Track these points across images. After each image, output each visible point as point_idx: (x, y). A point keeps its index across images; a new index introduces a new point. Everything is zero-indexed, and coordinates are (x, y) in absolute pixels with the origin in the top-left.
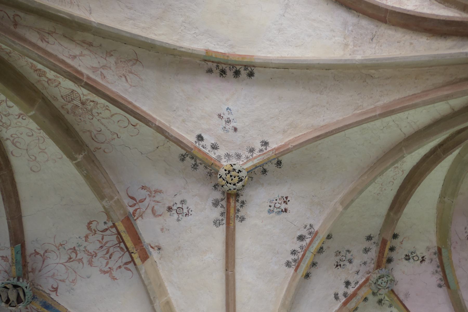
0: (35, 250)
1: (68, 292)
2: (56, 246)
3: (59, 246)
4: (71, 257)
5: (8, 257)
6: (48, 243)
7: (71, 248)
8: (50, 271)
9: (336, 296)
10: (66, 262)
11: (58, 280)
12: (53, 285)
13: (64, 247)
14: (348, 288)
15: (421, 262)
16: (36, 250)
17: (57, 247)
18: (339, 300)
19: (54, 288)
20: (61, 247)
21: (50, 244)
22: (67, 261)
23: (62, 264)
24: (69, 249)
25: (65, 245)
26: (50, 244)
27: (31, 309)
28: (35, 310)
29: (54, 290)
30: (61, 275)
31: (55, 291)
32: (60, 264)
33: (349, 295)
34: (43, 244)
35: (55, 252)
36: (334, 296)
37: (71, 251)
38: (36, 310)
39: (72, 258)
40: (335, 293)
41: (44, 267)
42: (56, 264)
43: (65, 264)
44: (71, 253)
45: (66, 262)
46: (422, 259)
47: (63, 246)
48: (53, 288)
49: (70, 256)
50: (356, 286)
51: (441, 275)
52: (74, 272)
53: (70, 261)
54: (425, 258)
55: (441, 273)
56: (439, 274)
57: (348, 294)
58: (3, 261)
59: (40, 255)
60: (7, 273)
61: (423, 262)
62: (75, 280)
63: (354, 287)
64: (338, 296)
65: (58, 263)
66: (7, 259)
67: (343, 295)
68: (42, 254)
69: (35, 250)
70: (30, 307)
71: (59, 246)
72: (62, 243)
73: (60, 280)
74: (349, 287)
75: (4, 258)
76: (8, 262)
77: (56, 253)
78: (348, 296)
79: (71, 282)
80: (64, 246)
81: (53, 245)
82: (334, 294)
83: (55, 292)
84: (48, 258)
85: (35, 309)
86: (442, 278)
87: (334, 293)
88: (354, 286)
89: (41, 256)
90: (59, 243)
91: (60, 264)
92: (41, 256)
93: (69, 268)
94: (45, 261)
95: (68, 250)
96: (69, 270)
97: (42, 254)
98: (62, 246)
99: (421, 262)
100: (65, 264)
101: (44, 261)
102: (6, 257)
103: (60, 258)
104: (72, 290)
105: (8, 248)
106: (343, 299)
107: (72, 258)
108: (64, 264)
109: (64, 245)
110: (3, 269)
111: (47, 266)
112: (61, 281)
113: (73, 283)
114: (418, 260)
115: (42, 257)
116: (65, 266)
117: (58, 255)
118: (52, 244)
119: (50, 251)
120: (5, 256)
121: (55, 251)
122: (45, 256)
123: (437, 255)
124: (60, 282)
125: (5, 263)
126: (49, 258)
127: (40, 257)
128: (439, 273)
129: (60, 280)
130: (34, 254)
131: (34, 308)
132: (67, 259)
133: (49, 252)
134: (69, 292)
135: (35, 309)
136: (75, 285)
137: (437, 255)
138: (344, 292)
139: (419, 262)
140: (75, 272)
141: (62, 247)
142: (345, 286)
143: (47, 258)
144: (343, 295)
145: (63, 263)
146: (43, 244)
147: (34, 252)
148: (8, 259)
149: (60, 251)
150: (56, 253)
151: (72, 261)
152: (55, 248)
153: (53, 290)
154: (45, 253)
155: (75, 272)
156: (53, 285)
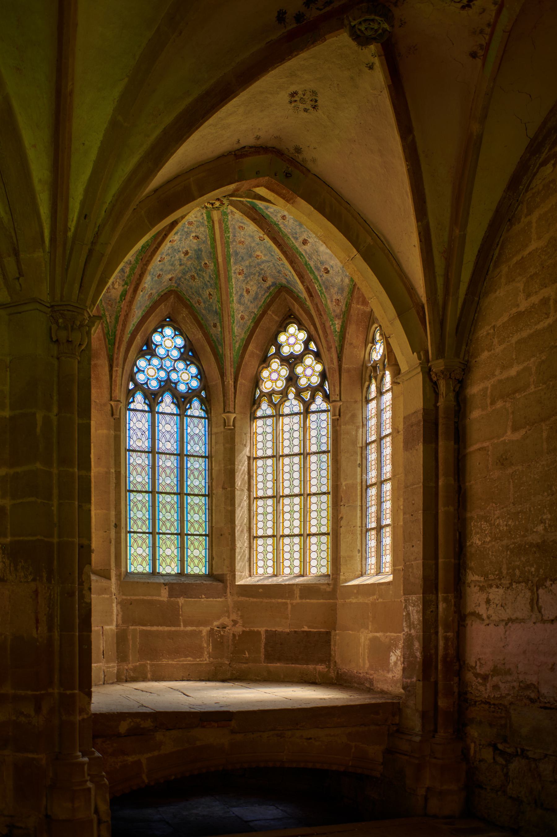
9: (281, 16)
14: (308, 8)
15: (463, 7)
18: (284, 24)
33: (305, 22)
36: (276, 14)
40: (280, 10)
46: (467, 3)
50: (324, 8)
51: (485, 39)
54: (474, 4)
55: (487, 37)
56: (484, 37)
57: (305, 17)
61: (467, 8)
63: (321, 10)
64: (284, 16)
67: (295, 17)
74: (311, 6)
78: (303, 23)
82: (278, 12)
86: (485, 45)
87: (279, 10)
88: (322, 7)
99: (463, 7)
106: (292, 25)
114: (459, 2)
123: (497, 6)
128: (485, 35)
137: (497, 6)
138: (298, 13)
139: (460, 5)
142: (304, 3)
144: (295, 17)
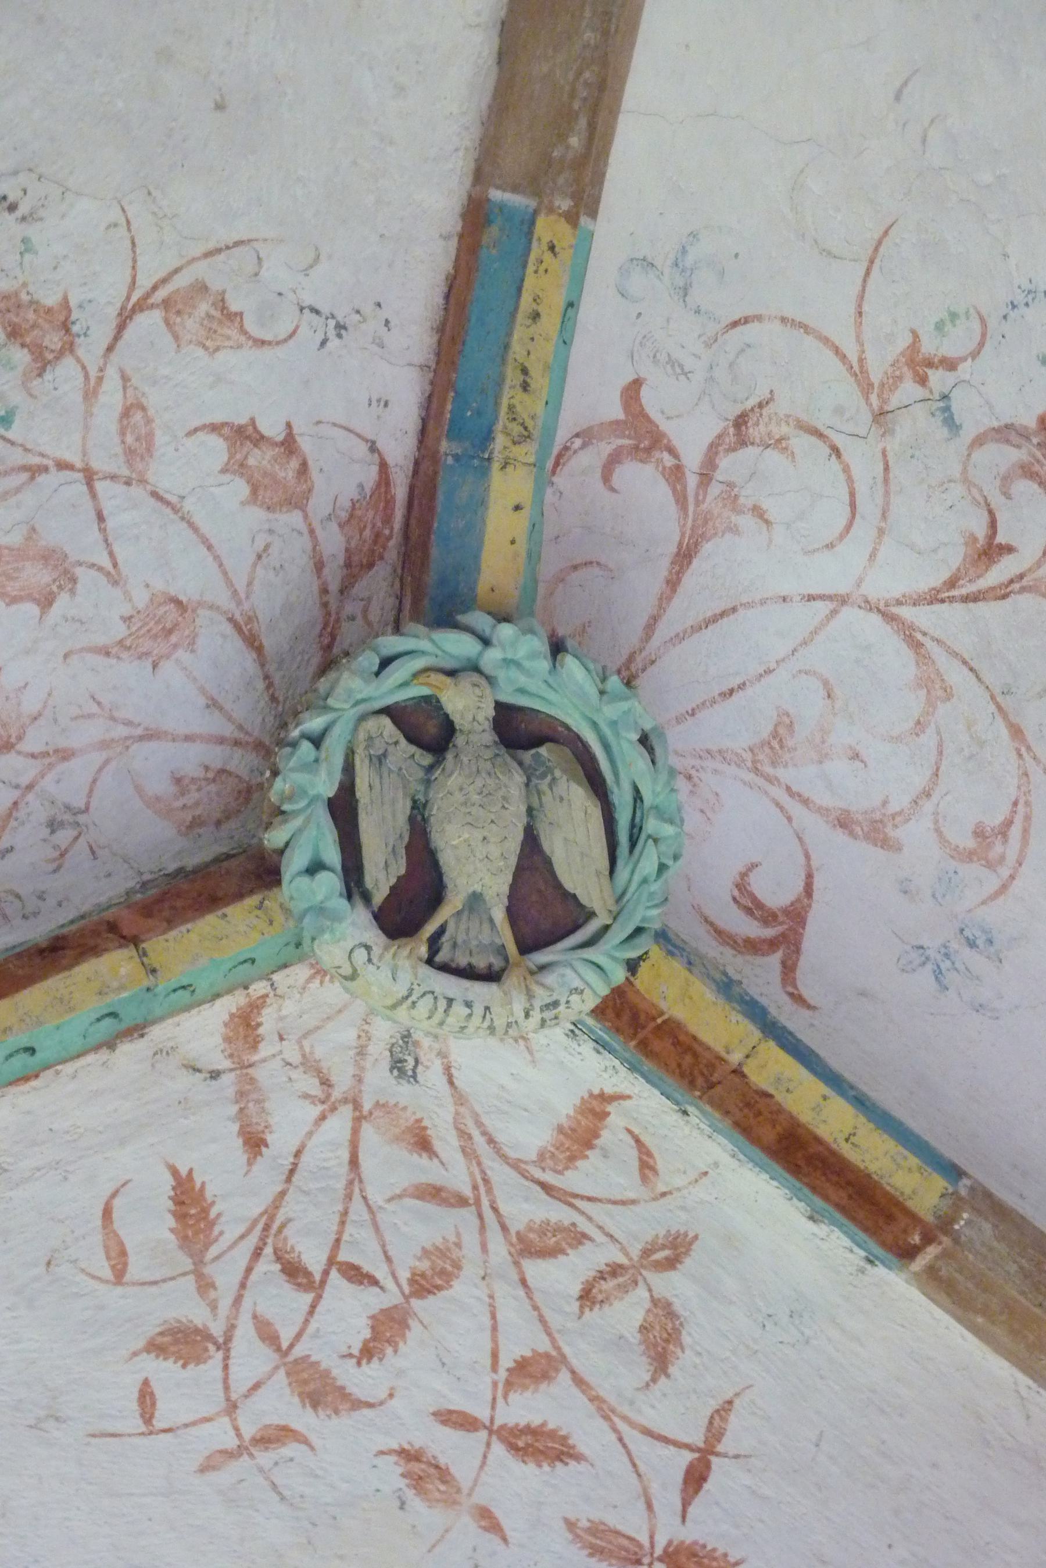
0: (632, 391)
1: (925, 977)
2: (860, 375)
3: (894, 381)
4: (1001, 539)
5: (305, 444)
6: (784, 320)
7: (1008, 427)
8: (742, 686)
10: (934, 598)
11: (823, 811)
12: (754, 866)
13: (945, 397)
16: (646, 395)
17: (866, 388)
19: (759, 905)
20: (909, 390)
21: (806, 328)
22: (952, 583)
23: (890, 618)
24: (997, 430)
25: (965, 369)
26: (809, 340)
27: (468, 1152)
28: (524, 1175)
29: (769, 933)
30: (856, 756)
31: (772, 944)
32: (868, 606)
34: (735, 324)
35: (836, 451)
37: (1013, 455)
38: (538, 1174)
39: (1009, 549)
41: (679, 638)
42: (822, 608)
43: (921, 617)
44: (1006, 480)
45: (934, 598)
47: (937, 378)
48: (754, 908)
49: (993, 525)
52: (1004, 733)
53: (983, 584)
58: (241, 488)
59: (668, 460)
60: (259, 650)
62: (1015, 832)
65: (843, 600)
66: (294, 464)
68: (692, 459)
69: (632, 391)
70: (464, 1135)
71: (894, 381)
72: (929, 347)
73: (844, 822)
75: (258, 458)
76: (297, 501)
77: (846, 470)
79: (969, 856)
80: (950, 378)
81: (837, 351)
83: (774, 960)
84: (746, 522)
85: (516, 1165)
89: (675, 475)
90: (903, 341)
91: (868, 606)
92: (675, 475)
93: (956, 676)
94: (707, 548)
95: (979, 441)
96: (948, 694)
97: (692, 459)
98: (923, 381)
100: (921, 617)
101: (685, 556)
102: (289, 444)
103: (881, 532)
104: (976, 960)
105: (340, 327)
107: (1009, 549)
108: (906, 612)
109: (950, 364)
110: (224, 599)
111: (715, 619)
112: (852, 834)
113: (990, 865)
115: (681, 500)
116: (916, 646)
117: (862, 490)
118: (826, 341)
119: (785, 429)
120: (272, 428)
121: (839, 440)
122: (715, 490)
124: (840, 837)
125: (257, 515)
126: (758, 512)
127: (662, 492)
129: (844, 822)
130: (605, 448)
131: (512, 1154)
132: (955, 557)
133: (780, 444)
134: (938, 974)
135: (516, 1165)
136: (1004, 888)
140: (1017, 732)
141: (919, 392)
143: (738, 511)
145: (899, 603)
146: (735, 324)
147: (616, 412)
148: (304, 469)
149: (893, 445)
150: (846, 470)
151: (1001, 593)
152: (846, 391)
153: (752, 929)
154: (732, 449)
155: (1017, 732)
156: (754, 866)
